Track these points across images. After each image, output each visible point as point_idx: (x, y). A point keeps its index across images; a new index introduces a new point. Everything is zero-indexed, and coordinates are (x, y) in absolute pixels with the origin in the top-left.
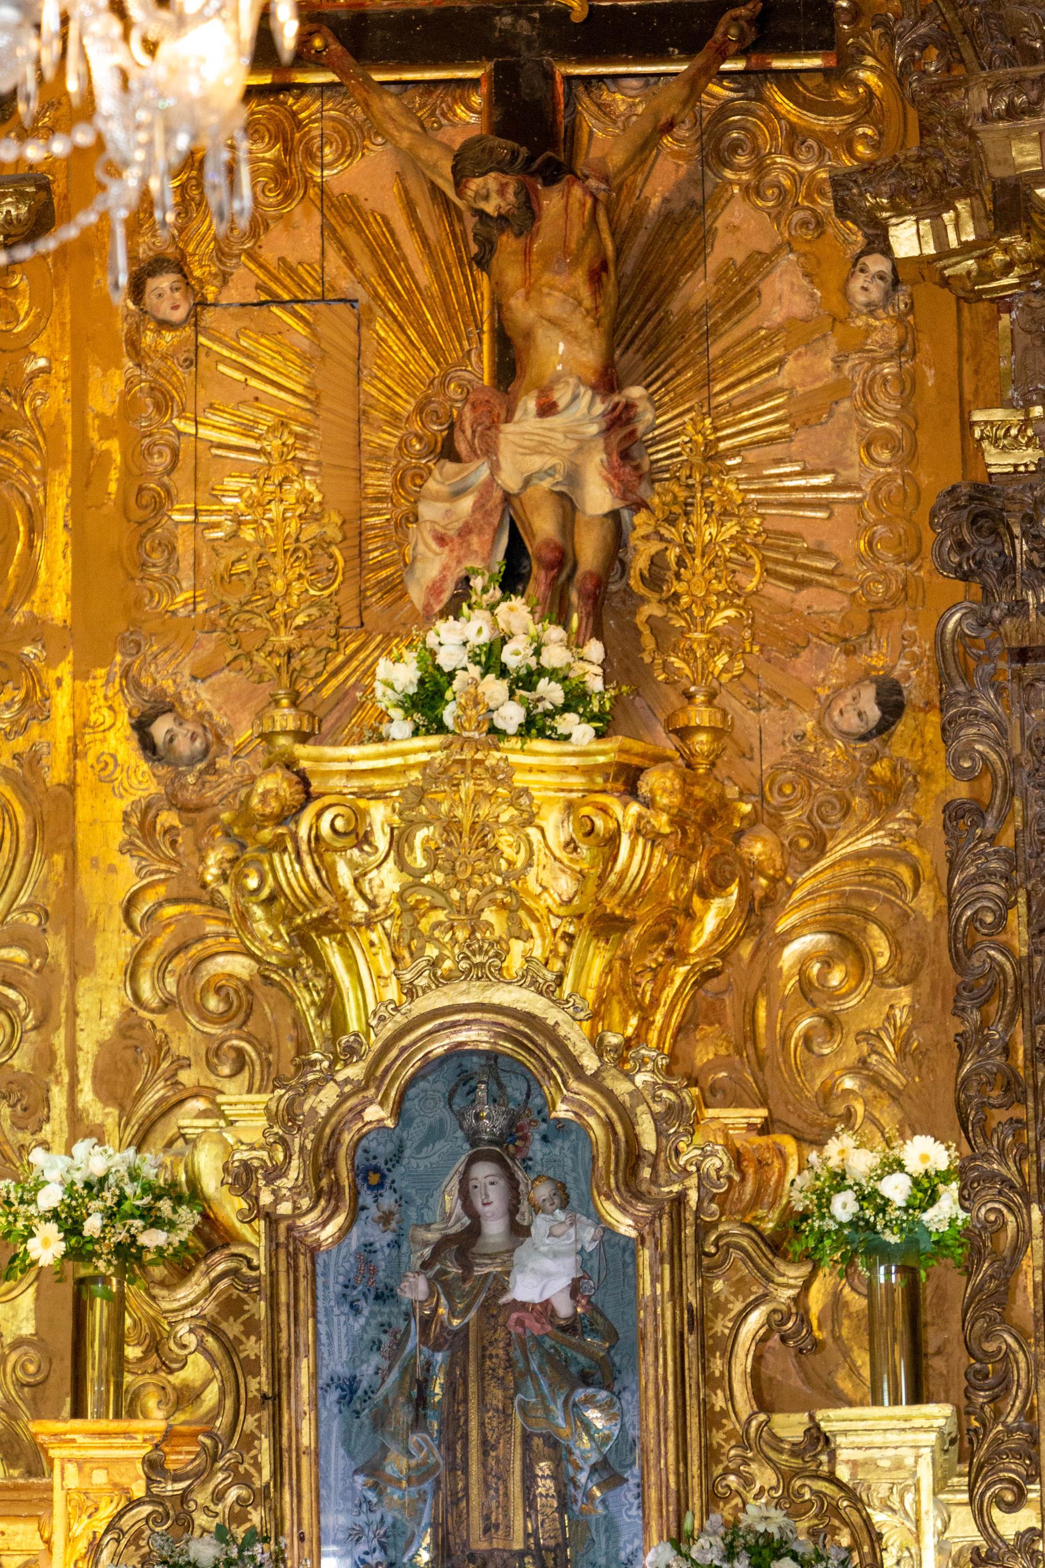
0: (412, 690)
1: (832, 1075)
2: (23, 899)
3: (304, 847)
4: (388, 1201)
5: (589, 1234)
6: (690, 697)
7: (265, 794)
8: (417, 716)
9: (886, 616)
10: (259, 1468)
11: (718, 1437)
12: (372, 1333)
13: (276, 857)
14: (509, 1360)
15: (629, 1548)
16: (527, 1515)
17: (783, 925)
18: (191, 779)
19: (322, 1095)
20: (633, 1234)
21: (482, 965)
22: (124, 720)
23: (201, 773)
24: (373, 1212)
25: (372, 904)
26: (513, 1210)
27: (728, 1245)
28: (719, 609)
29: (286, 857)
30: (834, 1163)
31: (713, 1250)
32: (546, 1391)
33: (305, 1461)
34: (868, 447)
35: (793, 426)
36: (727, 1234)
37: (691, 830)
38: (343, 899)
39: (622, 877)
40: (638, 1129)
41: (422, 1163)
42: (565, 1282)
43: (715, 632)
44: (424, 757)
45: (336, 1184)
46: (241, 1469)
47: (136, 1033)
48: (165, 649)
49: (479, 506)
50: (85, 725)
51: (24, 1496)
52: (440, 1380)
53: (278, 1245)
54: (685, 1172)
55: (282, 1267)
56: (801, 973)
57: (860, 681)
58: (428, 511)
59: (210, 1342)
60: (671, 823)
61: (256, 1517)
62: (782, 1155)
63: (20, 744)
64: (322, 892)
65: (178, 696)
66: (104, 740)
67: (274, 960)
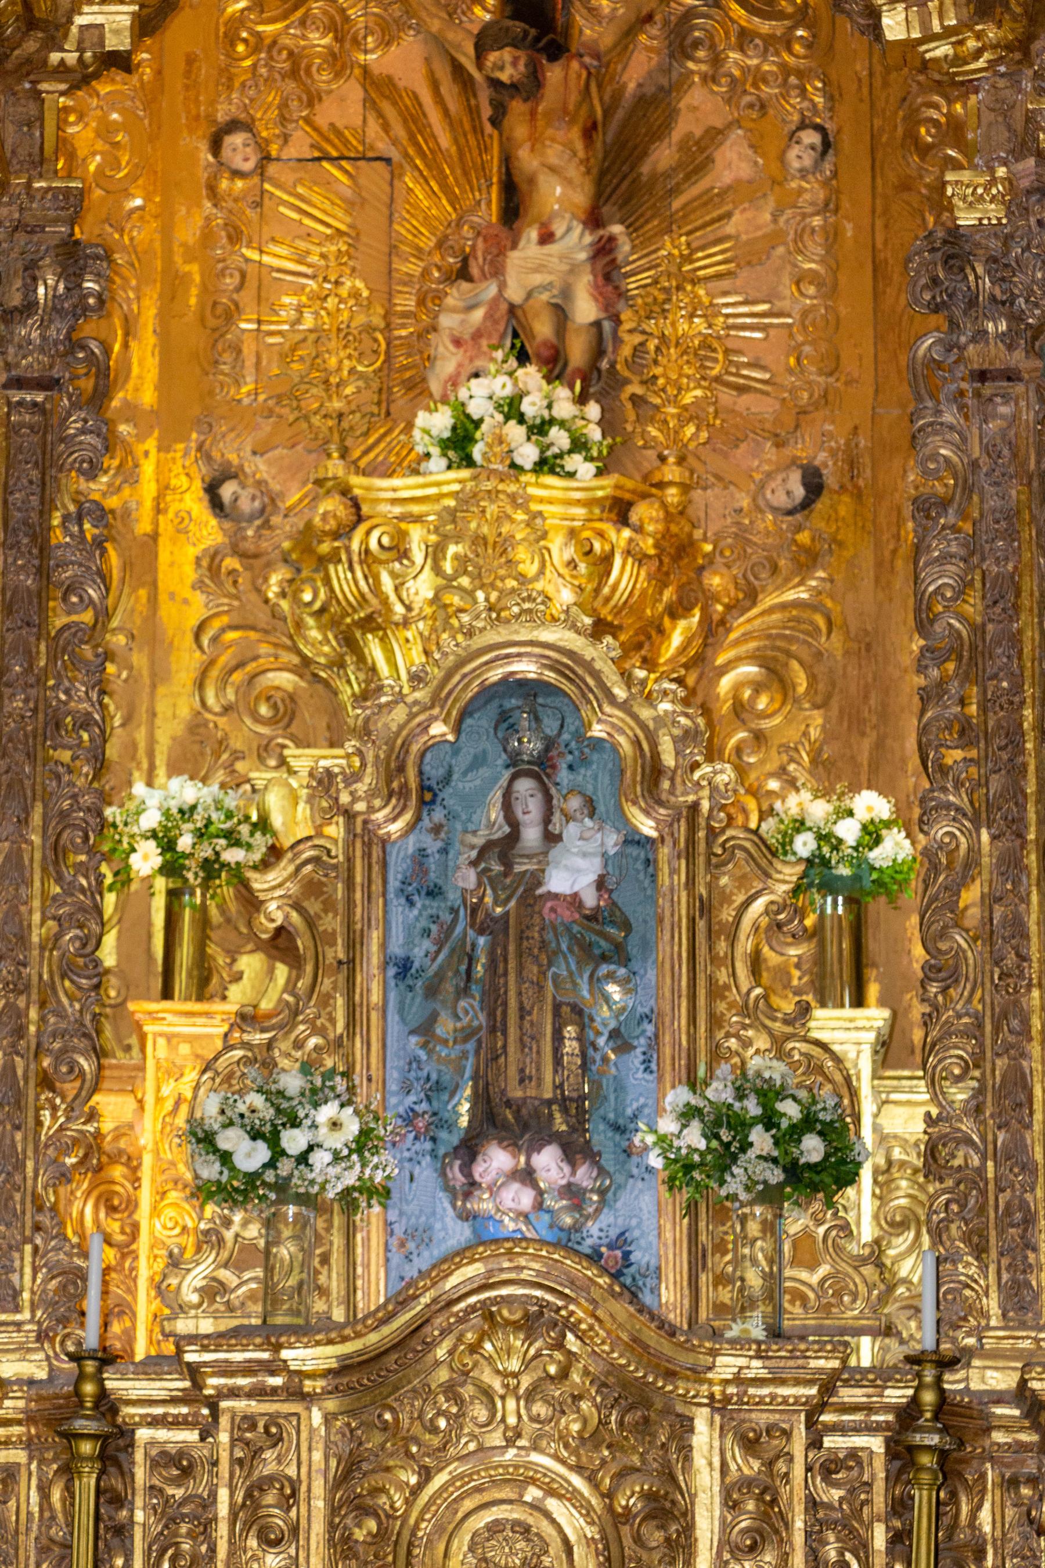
3: (355, 558)
4: (438, 815)
5: (612, 841)
6: (663, 459)
7: (325, 514)
8: (451, 453)
9: (809, 417)
10: (333, 1021)
11: (721, 1007)
12: (423, 923)
13: (331, 568)
15: (635, 1105)
16: (556, 1071)
17: (720, 661)
18: (250, 533)
20: (654, 834)
22: (198, 485)
23: (259, 528)
24: (426, 823)
25: (409, 608)
26: (547, 820)
27: (733, 847)
28: (688, 389)
29: (340, 568)
30: (794, 811)
31: (719, 851)
32: (573, 967)
33: (374, 1016)
34: (797, 283)
35: (738, 266)
36: (733, 838)
37: (666, 560)
38: (385, 602)
39: (614, 588)
41: (468, 785)
42: (592, 877)
43: (685, 408)
44: (456, 487)
45: (405, 786)
46: (319, 1022)
48: (232, 430)
49: (489, 316)
50: (167, 487)
55: (358, 853)
57: (788, 467)
58: (447, 321)
60: (656, 546)
64: (369, 596)
65: (241, 467)
66: (181, 500)
67: (322, 660)
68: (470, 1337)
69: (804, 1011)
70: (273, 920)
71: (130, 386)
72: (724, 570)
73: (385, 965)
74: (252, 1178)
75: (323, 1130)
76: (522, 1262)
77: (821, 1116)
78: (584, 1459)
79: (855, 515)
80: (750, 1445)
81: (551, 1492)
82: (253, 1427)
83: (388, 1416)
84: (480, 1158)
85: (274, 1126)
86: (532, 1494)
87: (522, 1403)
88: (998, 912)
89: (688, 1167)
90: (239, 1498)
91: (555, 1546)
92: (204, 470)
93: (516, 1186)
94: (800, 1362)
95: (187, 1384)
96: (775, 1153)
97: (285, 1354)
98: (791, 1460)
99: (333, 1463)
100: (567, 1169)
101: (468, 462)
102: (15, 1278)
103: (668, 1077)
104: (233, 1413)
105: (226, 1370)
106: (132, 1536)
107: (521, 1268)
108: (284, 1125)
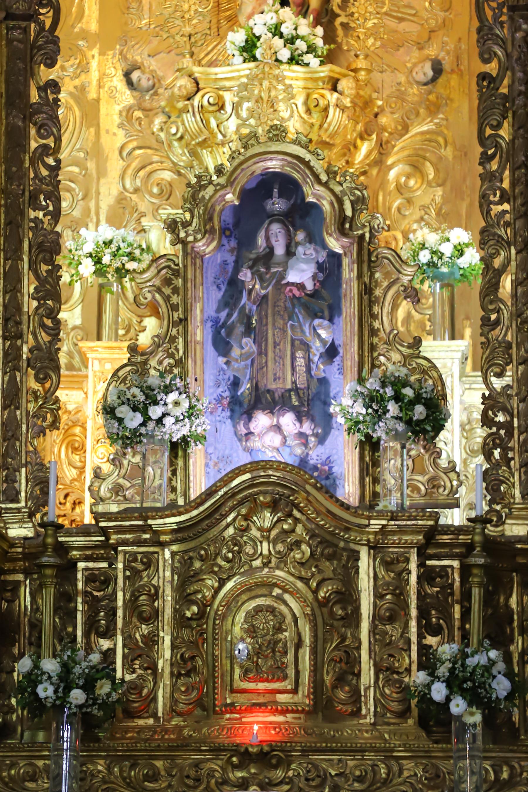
0: (243, 44)
1: (409, 224)
2: (78, 146)
3: (196, 110)
6: (357, 56)
7: (180, 87)
8: (245, 54)
9: (436, 33)
10: (177, 350)
11: (375, 340)
14: (286, 307)
15: (334, 392)
18: (147, 98)
19: (207, 190)
21: (277, 135)
22: (120, 73)
23: (152, 95)
24: (227, 247)
25: (224, 136)
28: (370, 20)
29: (188, 115)
30: (420, 239)
33: (198, 347)
37: (358, 109)
38: (212, 133)
39: (329, 125)
40: (345, 207)
43: (368, 29)
44: (248, 72)
45: (213, 229)
47: (123, 202)
48: (137, 44)
50: (104, 74)
51: (76, 379)
52: (255, 318)
53: (187, 254)
54: (364, 226)
55: (189, 263)
56: (398, 182)
59: (158, 296)
60: (351, 102)
61: (176, 371)
62: (395, 239)
63: (77, 82)
65: (142, 63)
66: (111, 81)
67: (182, 164)
68: (244, 511)
69: (417, 342)
70: (146, 298)
71: (84, 20)
72: (389, 115)
73: (203, 322)
74: (135, 431)
75: (170, 406)
76: (270, 472)
77: (424, 395)
78: (303, 573)
79: (459, 85)
80: (388, 565)
81: (285, 591)
82: (135, 560)
83: (203, 552)
84: (253, 420)
85: (145, 404)
86: (277, 591)
87: (271, 545)
88: (520, 290)
89: (357, 423)
90: (128, 597)
91: (289, 618)
92: (123, 65)
93: (272, 434)
94: (413, 522)
95: (103, 538)
96: (401, 415)
97: (150, 522)
98: (410, 573)
99: (176, 578)
100: (298, 425)
101: (254, 59)
102: (16, 485)
103: (349, 376)
104: (125, 553)
105: (120, 530)
106: (76, 618)
107: (269, 476)
108: (150, 404)
